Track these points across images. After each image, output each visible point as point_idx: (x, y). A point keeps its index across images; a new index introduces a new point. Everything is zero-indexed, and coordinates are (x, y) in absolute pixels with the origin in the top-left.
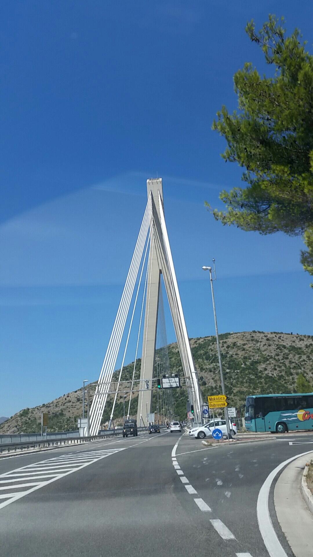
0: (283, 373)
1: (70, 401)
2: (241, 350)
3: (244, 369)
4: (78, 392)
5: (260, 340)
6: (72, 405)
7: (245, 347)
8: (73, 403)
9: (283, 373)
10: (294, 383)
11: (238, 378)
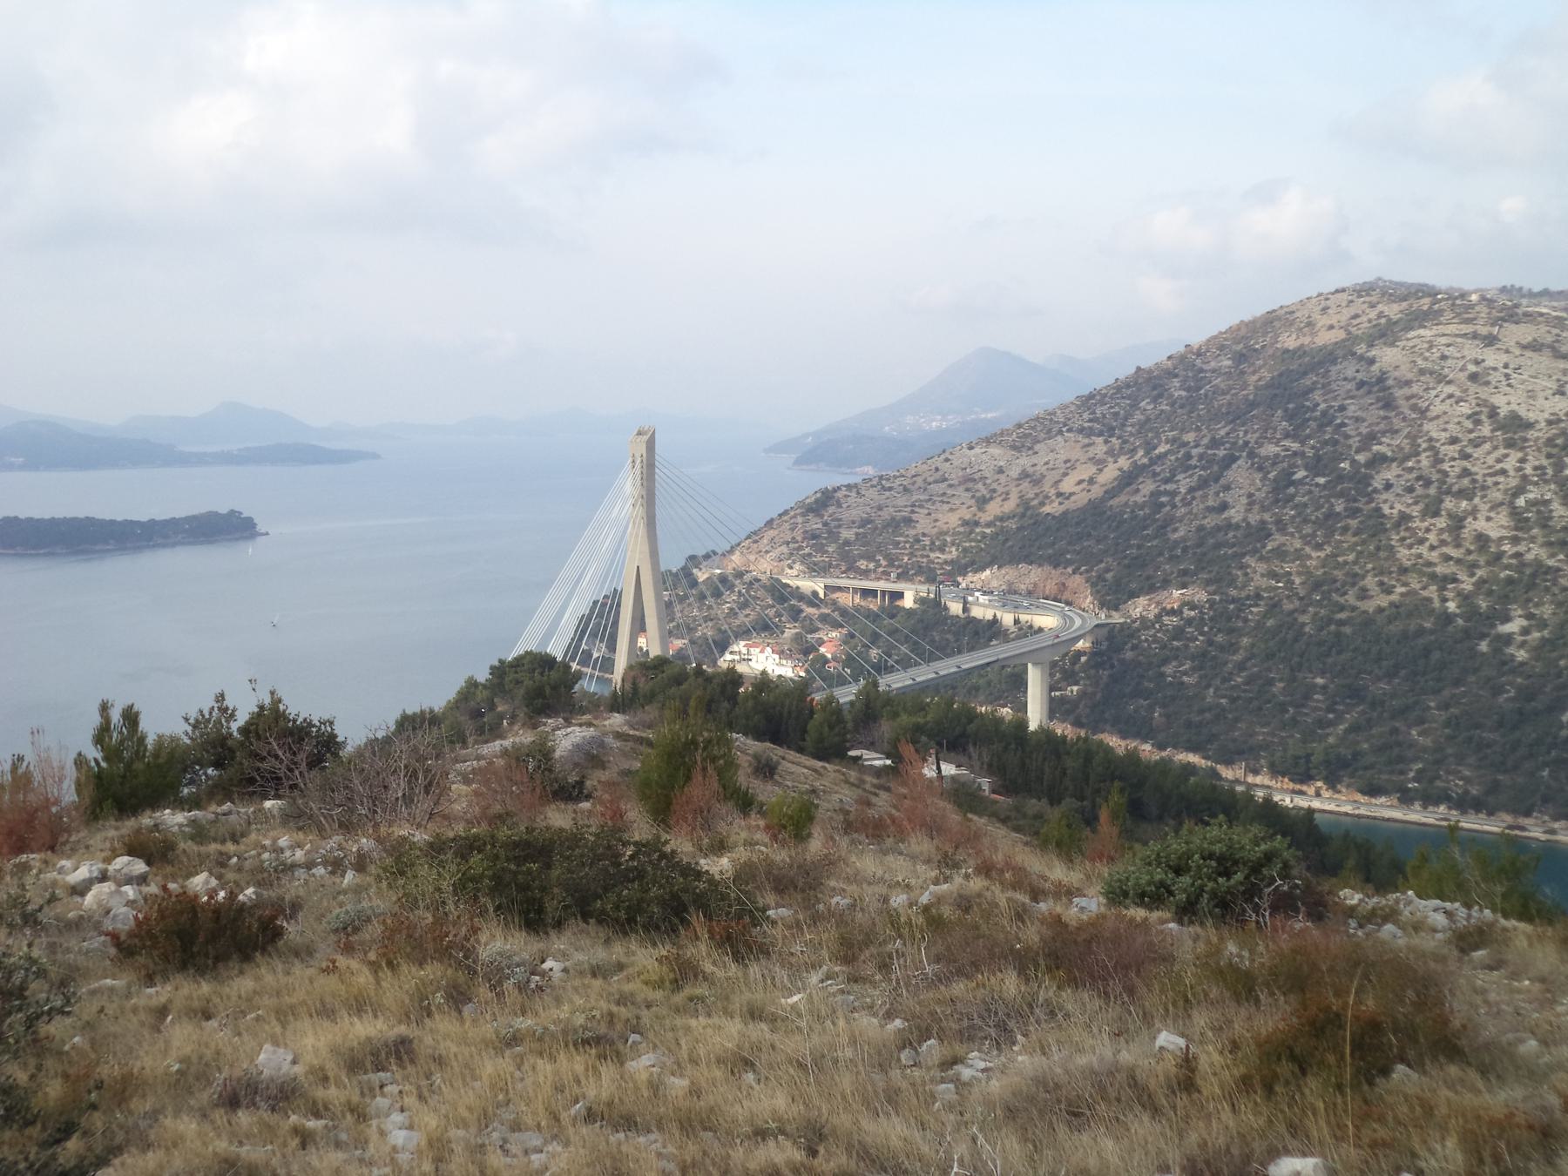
0: (1415, 511)
1: (946, 480)
2: (1380, 404)
3: (1341, 478)
4: (977, 450)
5: (1451, 376)
6: (944, 494)
7: (1399, 393)
8: (951, 486)
9: (1415, 511)
10: (1422, 541)
11: (1305, 505)
